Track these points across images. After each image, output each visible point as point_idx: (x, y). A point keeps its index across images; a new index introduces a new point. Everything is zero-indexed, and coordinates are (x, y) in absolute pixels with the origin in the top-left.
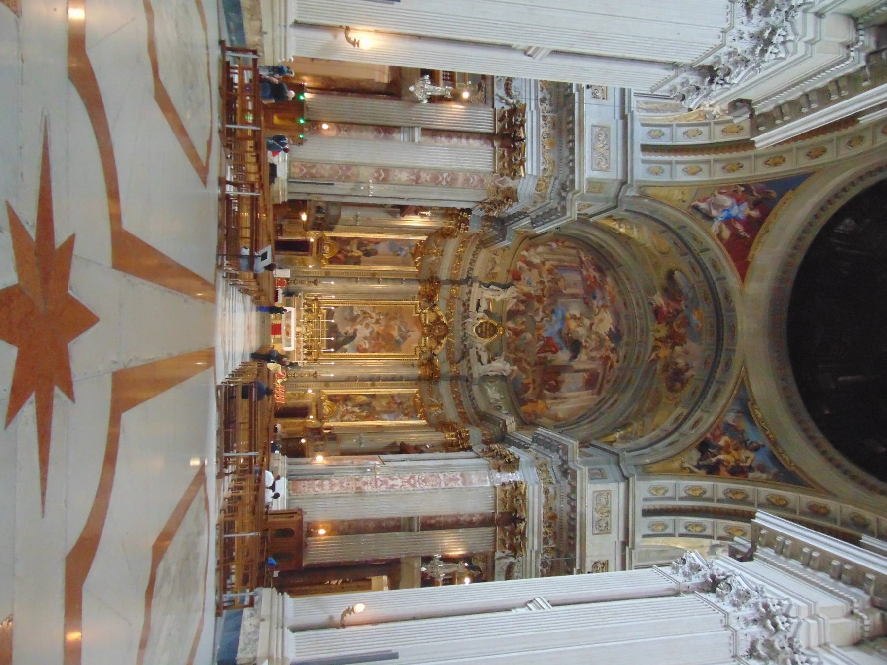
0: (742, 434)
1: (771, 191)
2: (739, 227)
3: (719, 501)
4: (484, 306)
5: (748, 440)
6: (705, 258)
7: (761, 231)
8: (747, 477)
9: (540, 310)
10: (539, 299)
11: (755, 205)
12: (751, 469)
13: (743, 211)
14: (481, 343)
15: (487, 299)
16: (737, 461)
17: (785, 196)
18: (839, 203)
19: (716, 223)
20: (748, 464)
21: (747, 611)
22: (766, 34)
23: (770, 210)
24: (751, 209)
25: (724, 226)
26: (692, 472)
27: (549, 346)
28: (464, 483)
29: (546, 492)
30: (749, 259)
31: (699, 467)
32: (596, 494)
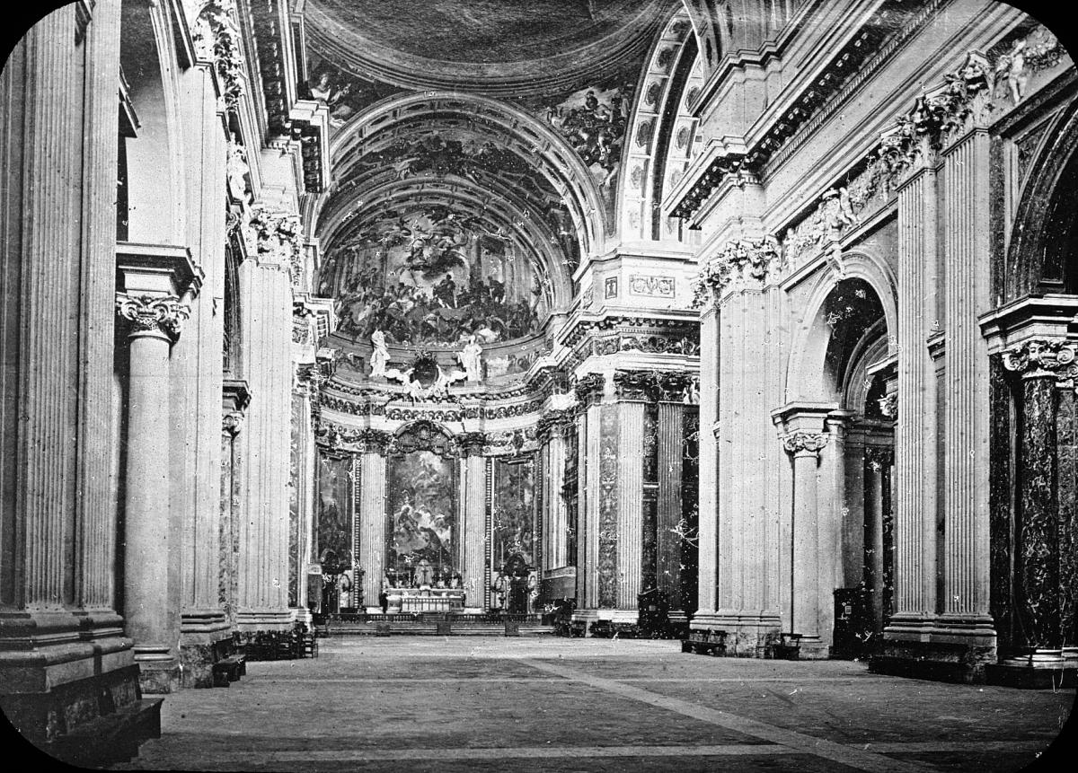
2: (336, 97)
3: (648, 153)
4: (394, 373)
6: (369, 132)
9: (399, 300)
10: (387, 301)
12: (617, 113)
14: (443, 379)
15: (387, 370)
21: (734, 273)
22: (283, 236)
25: (335, 113)
26: (615, 177)
27: (445, 291)
28: (613, 434)
29: (627, 348)
31: (610, 169)
32: (633, 292)
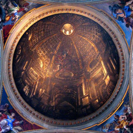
0: (112, 124)
1: (5, 104)
2: (17, 122)
5: (114, 120)
7: (21, 115)
8: (131, 113)
11: (10, 113)
13: (11, 118)
16: (125, 121)
17: (9, 100)
18: (17, 91)
19: (13, 130)
20: (125, 116)
23: (13, 109)
24: (11, 115)
25: (15, 128)
30: (33, 123)
